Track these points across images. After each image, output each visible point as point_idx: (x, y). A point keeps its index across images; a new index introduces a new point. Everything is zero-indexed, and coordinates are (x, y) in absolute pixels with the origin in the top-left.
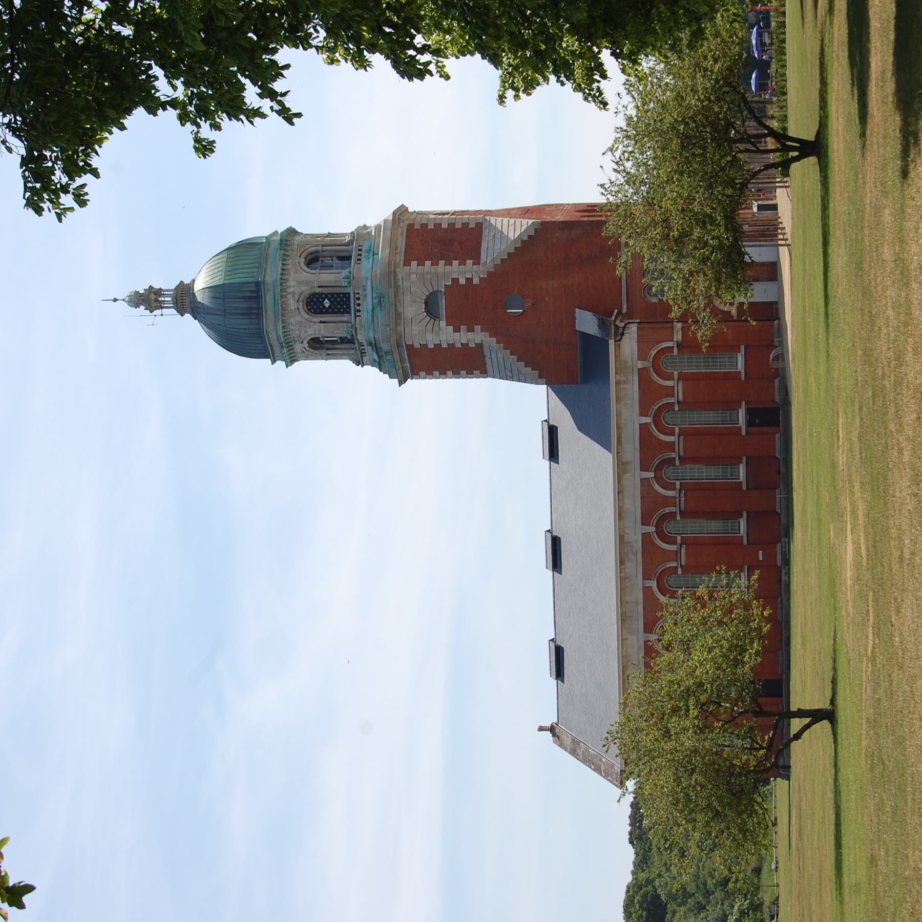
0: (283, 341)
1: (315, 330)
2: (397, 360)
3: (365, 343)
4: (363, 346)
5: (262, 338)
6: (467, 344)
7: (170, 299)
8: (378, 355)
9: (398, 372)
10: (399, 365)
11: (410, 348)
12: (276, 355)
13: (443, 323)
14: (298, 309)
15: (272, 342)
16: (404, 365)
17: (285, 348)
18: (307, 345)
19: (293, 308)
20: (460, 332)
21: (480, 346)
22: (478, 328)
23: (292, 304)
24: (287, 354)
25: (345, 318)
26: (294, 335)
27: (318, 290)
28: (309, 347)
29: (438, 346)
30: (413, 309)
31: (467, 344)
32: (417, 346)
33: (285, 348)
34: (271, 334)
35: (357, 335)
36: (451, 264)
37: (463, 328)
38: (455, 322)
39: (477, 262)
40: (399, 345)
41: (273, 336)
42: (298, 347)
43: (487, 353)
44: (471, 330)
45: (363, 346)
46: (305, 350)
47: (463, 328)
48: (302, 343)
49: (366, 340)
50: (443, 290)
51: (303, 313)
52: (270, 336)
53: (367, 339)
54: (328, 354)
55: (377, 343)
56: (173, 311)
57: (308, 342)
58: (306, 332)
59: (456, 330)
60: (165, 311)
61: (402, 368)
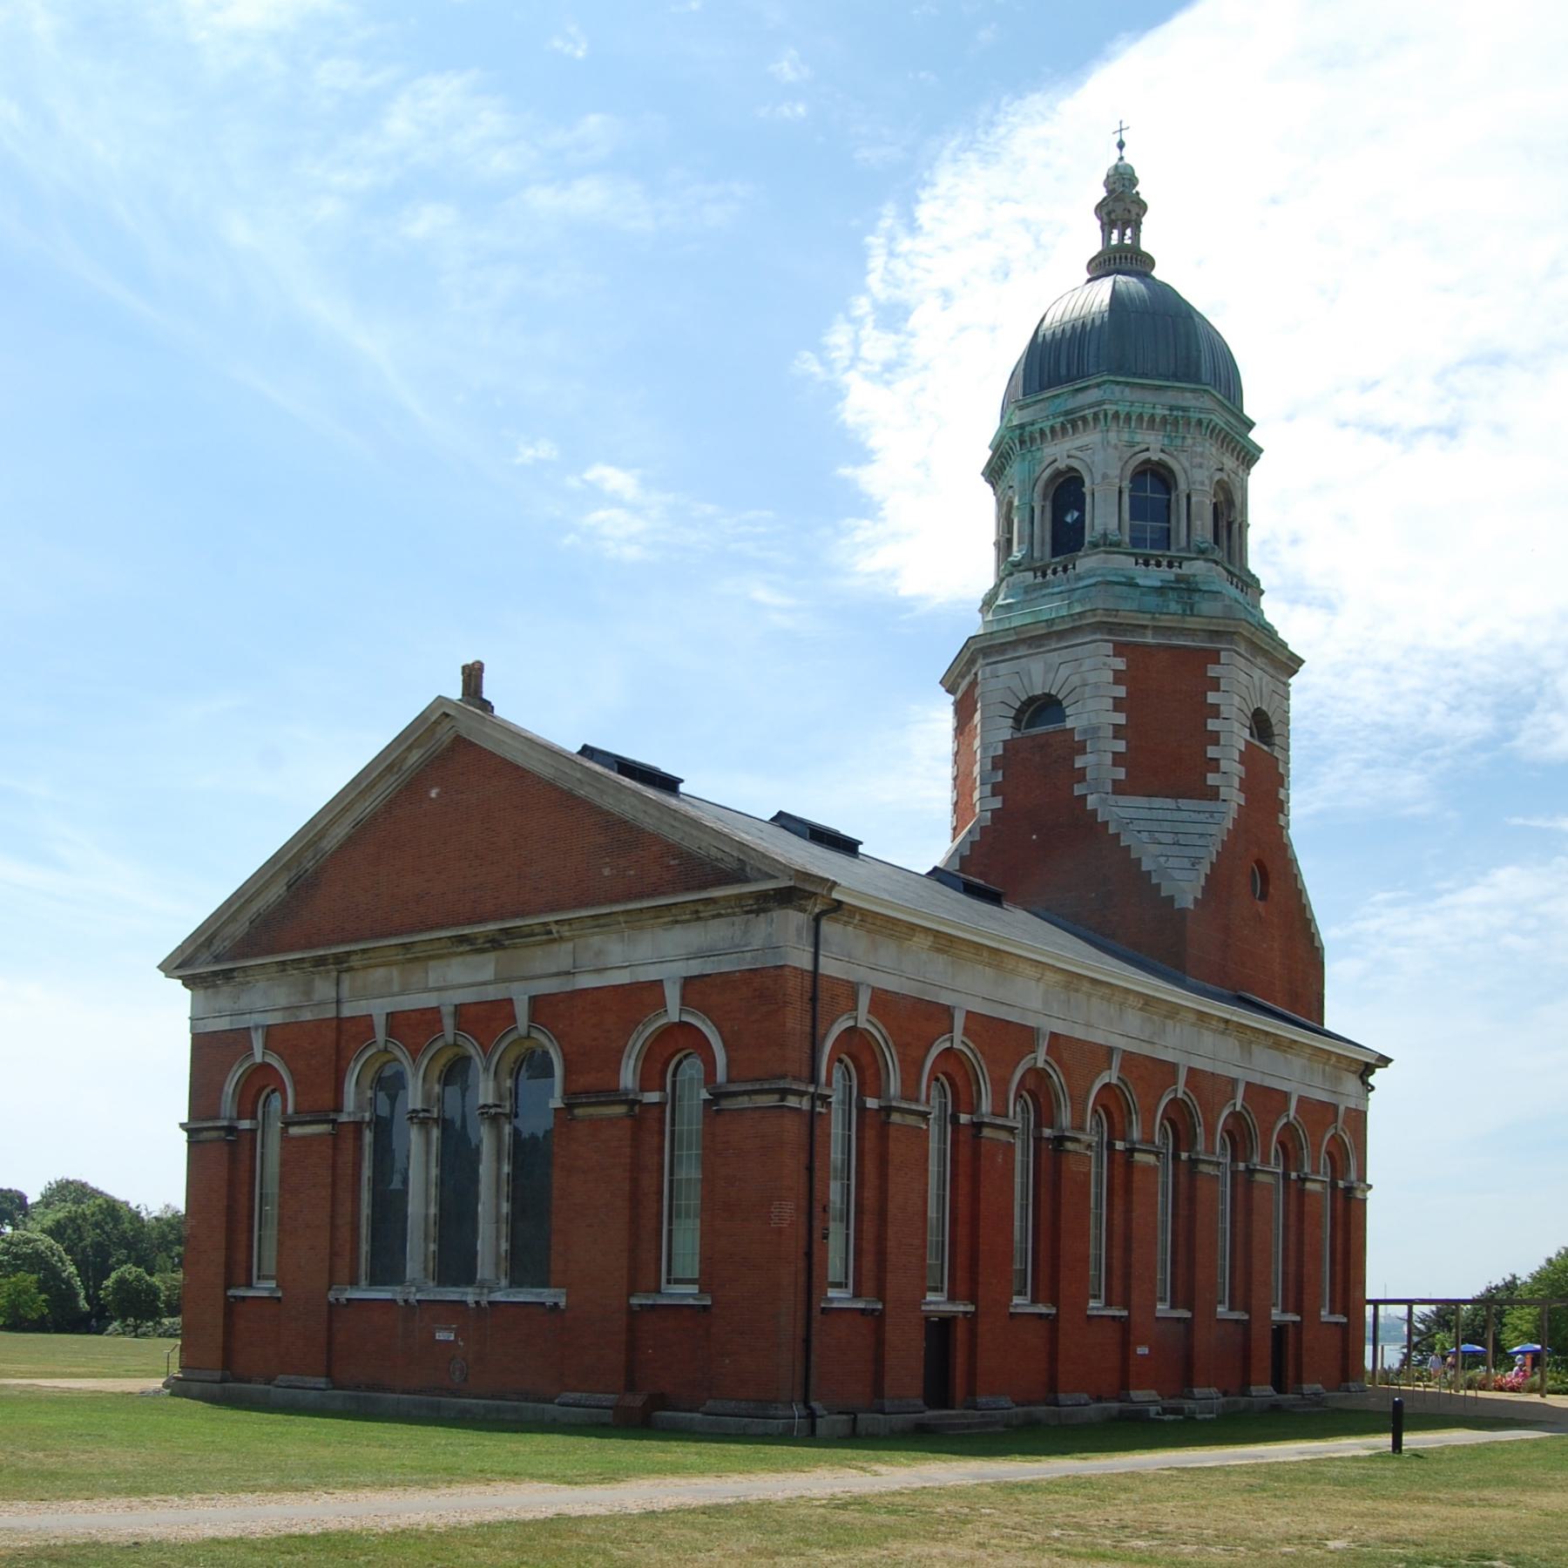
0: (1192, 414)
1: (1202, 483)
2: (1160, 620)
3: (1175, 570)
4: (1170, 565)
5: (1176, 378)
6: (1217, 770)
7: (1128, 242)
8: (1161, 588)
9: (1149, 616)
10: (1165, 621)
11: (1214, 656)
12: (1127, 390)
14: (1221, 470)
15: (1170, 393)
16: (1149, 633)
17: (1167, 412)
18: (1155, 458)
19: (1225, 460)
20: (1239, 763)
24: (1148, 411)
26: (1189, 441)
28: (1148, 461)
29: (1215, 711)
31: (1217, 770)
32: (1213, 671)
33: (1167, 412)
34: (1197, 399)
35: (1207, 560)
40: (1215, 635)
41: (1188, 400)
43: (1184, 803)
45: (1170, 565)
46: (1137, 449)
48: (1162, 451)
49: (1195, 576)
52: (1188, 395)
53: (1197, 578)
54: (1120, 492)
55: (1206, 595)
57: (1161, 464)
58: (1201, 466)
61: (1145, 627)
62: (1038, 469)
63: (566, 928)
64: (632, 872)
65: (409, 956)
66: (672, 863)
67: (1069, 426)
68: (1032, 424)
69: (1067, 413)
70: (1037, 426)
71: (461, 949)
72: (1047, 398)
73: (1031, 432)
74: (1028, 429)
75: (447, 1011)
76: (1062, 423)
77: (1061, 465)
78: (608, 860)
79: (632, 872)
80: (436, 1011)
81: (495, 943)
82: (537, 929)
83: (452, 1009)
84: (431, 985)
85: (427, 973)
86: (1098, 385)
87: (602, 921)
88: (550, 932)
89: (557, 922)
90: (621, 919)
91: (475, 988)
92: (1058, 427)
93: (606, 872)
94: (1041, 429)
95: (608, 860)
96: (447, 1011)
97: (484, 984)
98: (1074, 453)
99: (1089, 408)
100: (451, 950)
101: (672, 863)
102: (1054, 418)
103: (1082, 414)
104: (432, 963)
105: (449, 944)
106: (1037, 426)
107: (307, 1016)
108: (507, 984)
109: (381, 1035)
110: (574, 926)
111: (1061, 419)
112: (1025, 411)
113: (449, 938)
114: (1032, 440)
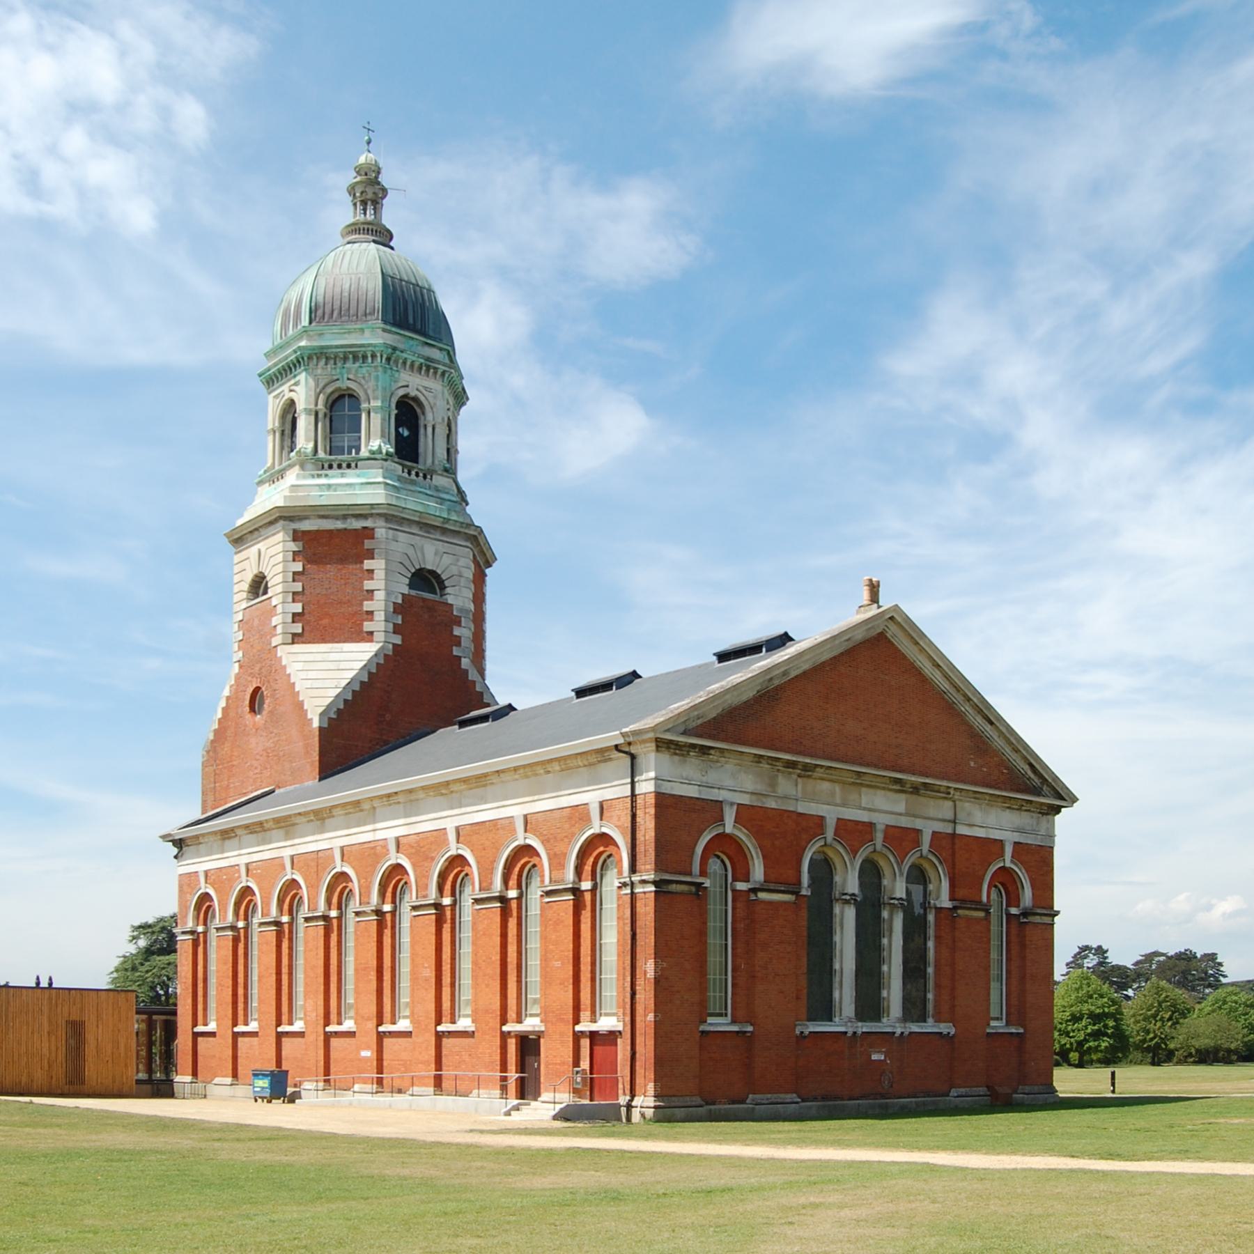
62: (394, 386)
63: (958, 793)
64: (985, 770)
65: (858, 781)
66: (1005, 771)
67: (424, 368)
68: (402, 352)
69: (428, 359)
70: (405, 355)
71: (894, 787)
72: (405, 336)
73: (398, 356)
74: (397, 352)
75: (880, 827)
76: (421, 364)
77: (413, 393)
78: (972, 756)
79: (985, 770)
80: (871, 825)
81: (916, 790)
82: (942, 789)
83: (883, 827)
84: (863, 805)
85: (860, 796)
86: (441, 349)
87: (977, 796)
88: (949, 793)
89: (955, 789)
90: (987, 797)
91: (893, 816)
92: (417, 364)
93: (972, 764)
94: (406, 359)
95: (972, 756)
96: (880, 827)
97: (900, 814)
98: (420, 388)
99: (443, 365)
100: (887, 786)
101: (1005, 771)
102: (418, 357)
103: (437, 366)
104: (864, 790)
105: (888, 782)
106: (405, 355)
107: (772, 804)
108: (913, 819)
109: (830, 833)
110: (963, 794)
111: (422, 361)
112: (386, 334)
113: (890, 777)
114: (396, 362)
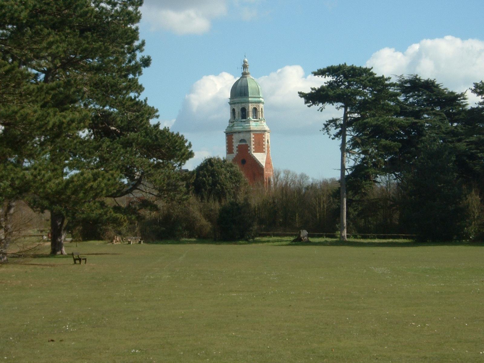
11: (232, 135)
13: (239, 144)
21: (233, 153)
22: (237, 153)
23: (243, 105)
25: (240, 118)
27: (247, 111)
30: (241, 136)
36: (253, 145)
37: (237, 149)
38: (239, 147)
39: (254, 152)
42: (233, 106)
44: (237, 151)
47: (237, 149)
50: (247, 143)
51: (241, 107)
56: (242, 72)
59: (237, 147)
60: (242, 69)
